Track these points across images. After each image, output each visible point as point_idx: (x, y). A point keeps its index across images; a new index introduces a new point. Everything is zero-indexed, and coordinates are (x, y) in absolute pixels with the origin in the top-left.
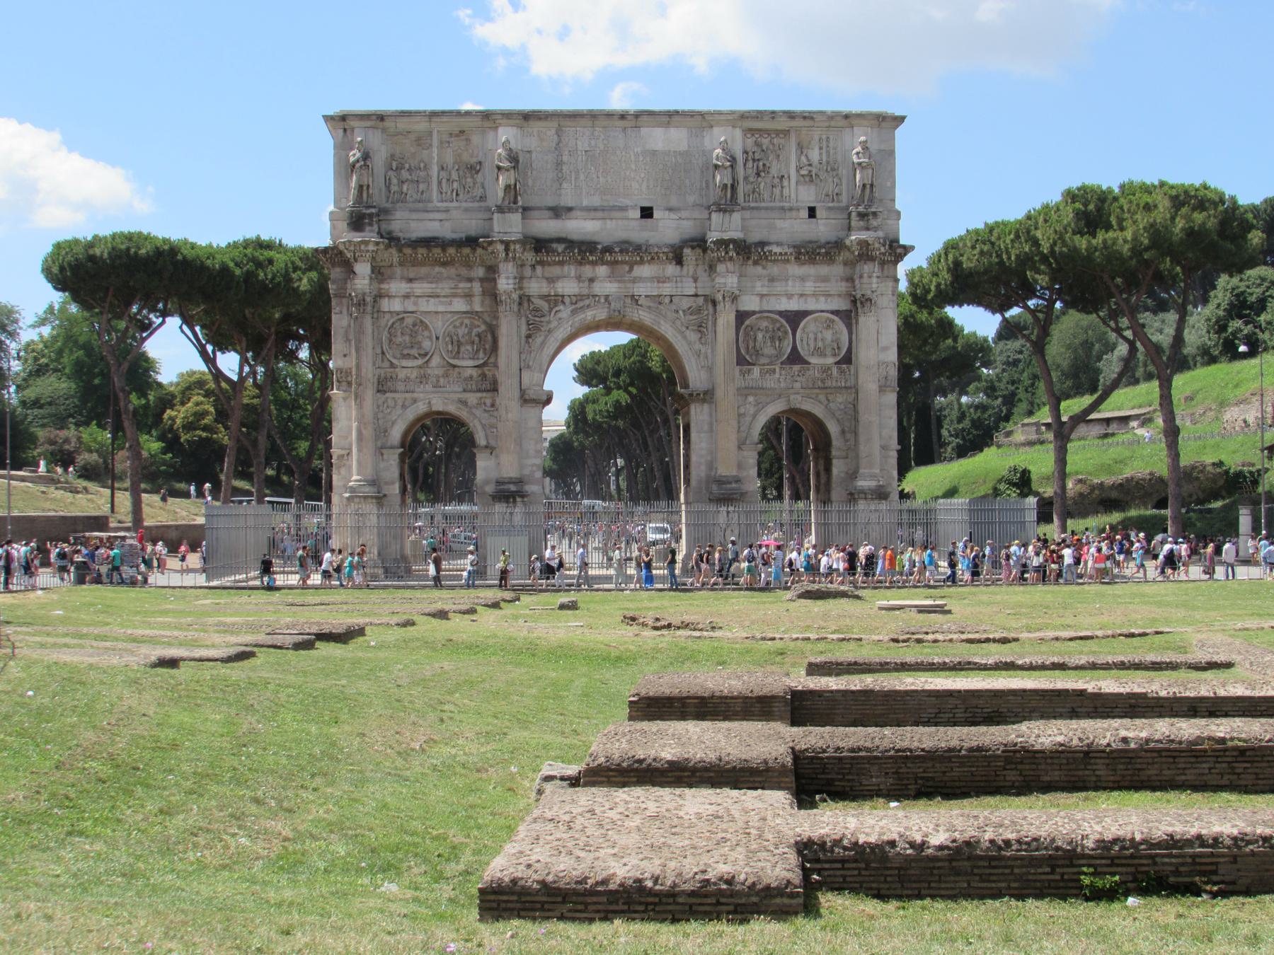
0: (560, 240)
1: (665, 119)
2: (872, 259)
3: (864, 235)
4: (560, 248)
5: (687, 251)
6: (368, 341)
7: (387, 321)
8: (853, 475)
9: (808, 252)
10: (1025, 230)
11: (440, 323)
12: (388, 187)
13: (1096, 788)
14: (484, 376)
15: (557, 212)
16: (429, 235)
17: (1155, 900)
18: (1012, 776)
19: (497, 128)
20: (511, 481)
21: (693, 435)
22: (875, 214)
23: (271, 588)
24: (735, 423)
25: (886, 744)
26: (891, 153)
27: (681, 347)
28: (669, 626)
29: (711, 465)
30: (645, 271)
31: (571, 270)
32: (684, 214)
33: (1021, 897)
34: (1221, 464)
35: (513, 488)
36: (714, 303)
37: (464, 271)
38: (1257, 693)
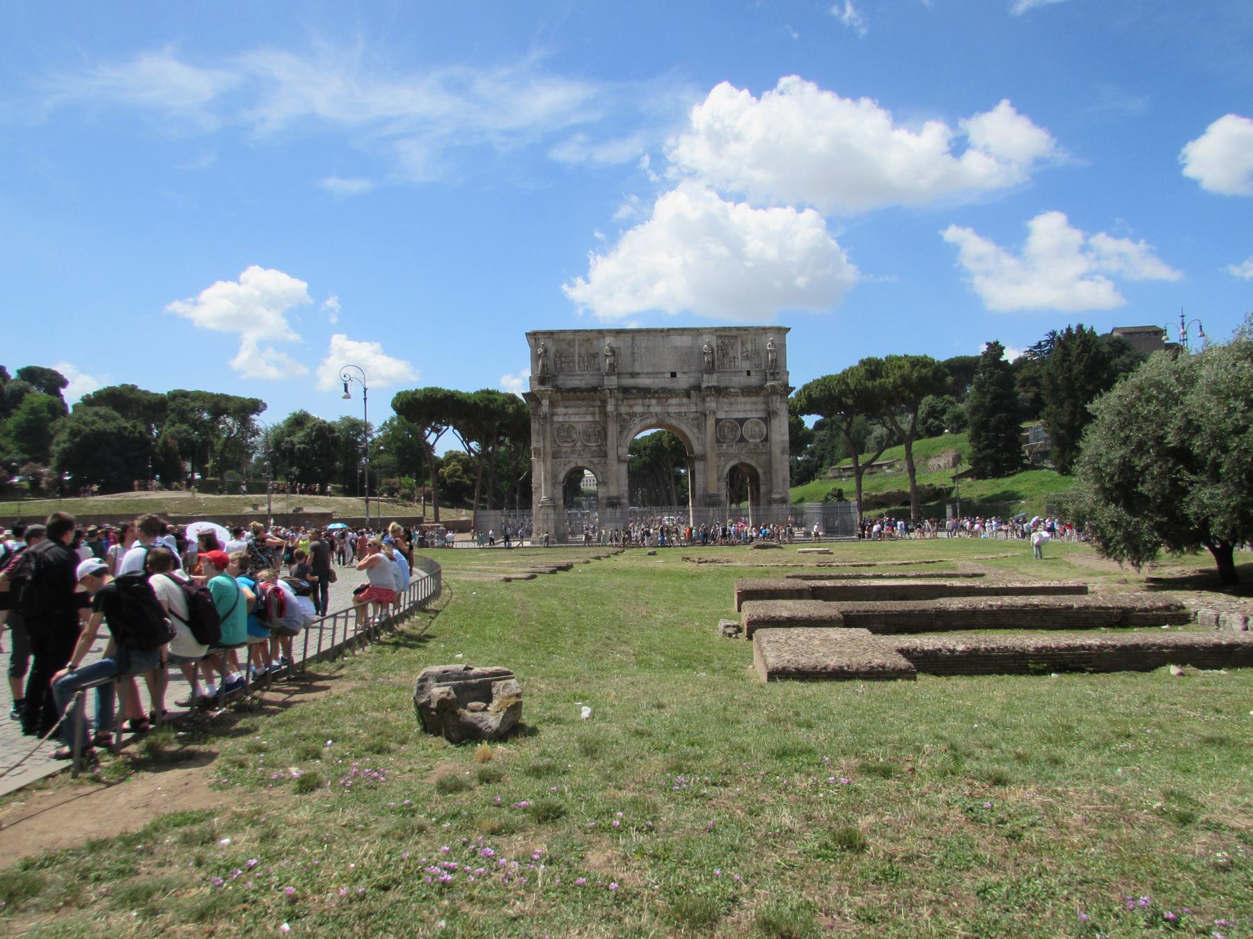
0: (634, 388)
2: (777, 394)
3: (773, 383)
4: (635, 391)
6: (548, 434)
7: (556, 426)
8: (770, 492)
9: (747, 391)
10: (842, 378)
12: (556, 365)
13: (979, 628)
15: (633, 375)
17: (1064, 675)
18: (939, 623)
20: (614, 498)
21: (697, 475)
23: (510, 548)
25: (880, 609)
26: (784, 345)
27: (690, 436)
28: (706, 562)
29: (705, 489)
30: (673, 401)
31: (640, 401)
33: (1000, 674)
34: (932, 485)
36: (705, 415)
37: (591, 403)
38: (1027, 586)
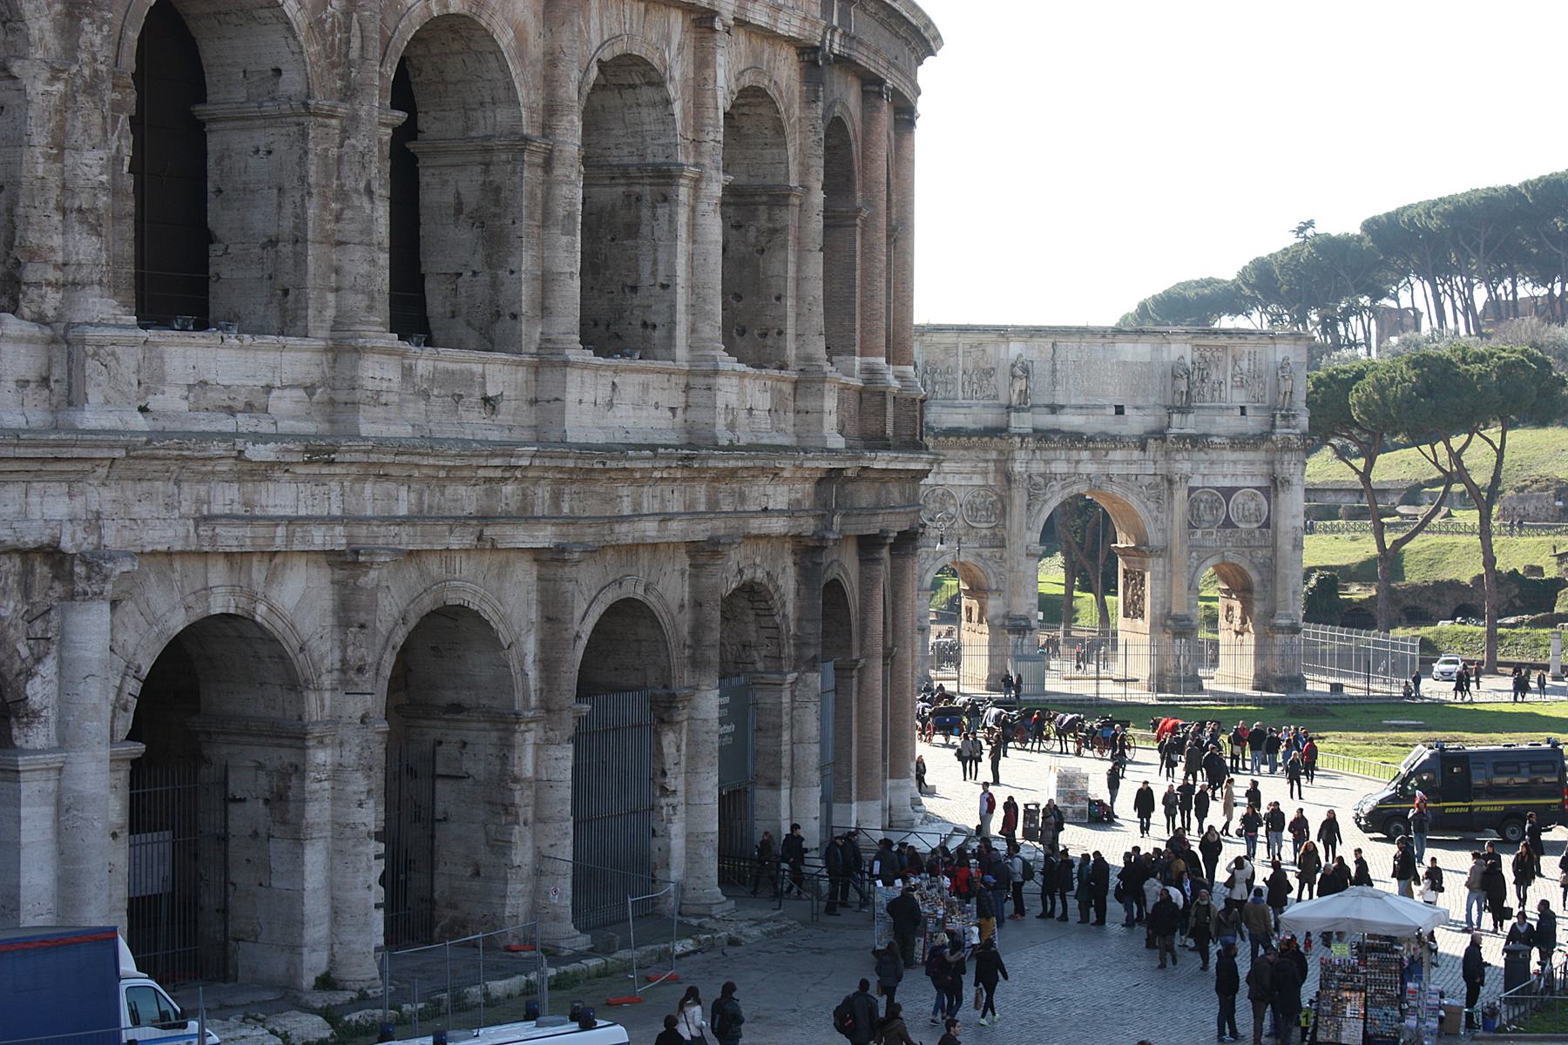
1: (1135, 337)
5: (1151, 441)
8: (1272, 613)
9: (1239, 442)
11: (963, 495)
14: (995, 535)
16: (956, 425)
19: (1008, 342)
22: (1293, 416)
24: (1186, 574)
27: (1143, 514)
30: (1117, 455)
31: (1063, 454)
32: (1148, 411)
35: (1023, 623)
37: (981, 454)
